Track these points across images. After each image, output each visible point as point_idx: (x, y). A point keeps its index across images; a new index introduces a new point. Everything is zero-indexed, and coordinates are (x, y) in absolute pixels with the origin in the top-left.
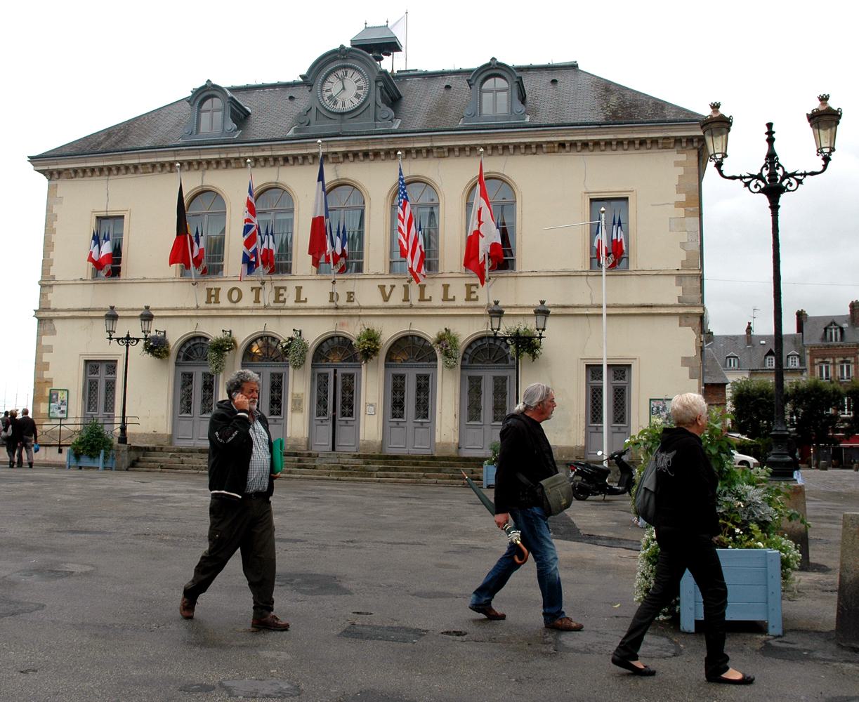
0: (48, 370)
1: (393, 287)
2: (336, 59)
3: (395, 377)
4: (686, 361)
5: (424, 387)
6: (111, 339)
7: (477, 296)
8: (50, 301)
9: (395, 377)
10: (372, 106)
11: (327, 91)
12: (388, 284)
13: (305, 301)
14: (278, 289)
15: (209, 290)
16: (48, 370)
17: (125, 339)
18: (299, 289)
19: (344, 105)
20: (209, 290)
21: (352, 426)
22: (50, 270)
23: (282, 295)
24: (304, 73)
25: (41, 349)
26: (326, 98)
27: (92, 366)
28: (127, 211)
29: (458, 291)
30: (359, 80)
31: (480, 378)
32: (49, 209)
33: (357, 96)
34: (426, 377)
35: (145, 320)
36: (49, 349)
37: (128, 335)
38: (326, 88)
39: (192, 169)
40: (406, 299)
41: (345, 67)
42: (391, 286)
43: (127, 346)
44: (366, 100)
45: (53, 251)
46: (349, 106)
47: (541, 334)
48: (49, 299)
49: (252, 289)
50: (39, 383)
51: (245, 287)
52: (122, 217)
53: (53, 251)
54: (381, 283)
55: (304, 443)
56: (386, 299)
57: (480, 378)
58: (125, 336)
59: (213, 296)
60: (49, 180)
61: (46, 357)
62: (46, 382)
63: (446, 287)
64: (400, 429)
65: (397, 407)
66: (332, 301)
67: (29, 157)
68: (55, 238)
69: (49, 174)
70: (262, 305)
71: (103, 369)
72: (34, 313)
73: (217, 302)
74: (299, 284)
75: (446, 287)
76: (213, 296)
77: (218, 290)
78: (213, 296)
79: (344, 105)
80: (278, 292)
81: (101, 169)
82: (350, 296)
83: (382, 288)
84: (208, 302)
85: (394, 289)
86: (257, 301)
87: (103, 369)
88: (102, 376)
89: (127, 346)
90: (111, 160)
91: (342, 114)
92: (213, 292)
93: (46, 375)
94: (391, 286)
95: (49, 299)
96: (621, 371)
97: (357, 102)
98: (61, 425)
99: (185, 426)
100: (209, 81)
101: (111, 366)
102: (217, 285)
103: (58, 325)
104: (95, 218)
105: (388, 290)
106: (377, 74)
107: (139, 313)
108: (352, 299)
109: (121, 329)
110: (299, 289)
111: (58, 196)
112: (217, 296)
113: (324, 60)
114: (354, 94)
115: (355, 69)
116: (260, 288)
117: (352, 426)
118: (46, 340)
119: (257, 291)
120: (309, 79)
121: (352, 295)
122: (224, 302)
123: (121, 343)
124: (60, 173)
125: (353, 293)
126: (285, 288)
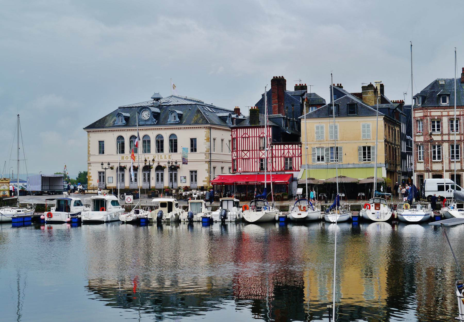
4: (206, 170)
5: (162, 175)
27: (100, 173)
29: (167, 156)
68: (90, 146)
71: (102, 173)
78: (123, 158)
87: (102, 173)
96: (196, 172)
97: (148, 118)
101: (103, 173)
103: (92, 164)
118: (90, 168)
122: (125, 159)
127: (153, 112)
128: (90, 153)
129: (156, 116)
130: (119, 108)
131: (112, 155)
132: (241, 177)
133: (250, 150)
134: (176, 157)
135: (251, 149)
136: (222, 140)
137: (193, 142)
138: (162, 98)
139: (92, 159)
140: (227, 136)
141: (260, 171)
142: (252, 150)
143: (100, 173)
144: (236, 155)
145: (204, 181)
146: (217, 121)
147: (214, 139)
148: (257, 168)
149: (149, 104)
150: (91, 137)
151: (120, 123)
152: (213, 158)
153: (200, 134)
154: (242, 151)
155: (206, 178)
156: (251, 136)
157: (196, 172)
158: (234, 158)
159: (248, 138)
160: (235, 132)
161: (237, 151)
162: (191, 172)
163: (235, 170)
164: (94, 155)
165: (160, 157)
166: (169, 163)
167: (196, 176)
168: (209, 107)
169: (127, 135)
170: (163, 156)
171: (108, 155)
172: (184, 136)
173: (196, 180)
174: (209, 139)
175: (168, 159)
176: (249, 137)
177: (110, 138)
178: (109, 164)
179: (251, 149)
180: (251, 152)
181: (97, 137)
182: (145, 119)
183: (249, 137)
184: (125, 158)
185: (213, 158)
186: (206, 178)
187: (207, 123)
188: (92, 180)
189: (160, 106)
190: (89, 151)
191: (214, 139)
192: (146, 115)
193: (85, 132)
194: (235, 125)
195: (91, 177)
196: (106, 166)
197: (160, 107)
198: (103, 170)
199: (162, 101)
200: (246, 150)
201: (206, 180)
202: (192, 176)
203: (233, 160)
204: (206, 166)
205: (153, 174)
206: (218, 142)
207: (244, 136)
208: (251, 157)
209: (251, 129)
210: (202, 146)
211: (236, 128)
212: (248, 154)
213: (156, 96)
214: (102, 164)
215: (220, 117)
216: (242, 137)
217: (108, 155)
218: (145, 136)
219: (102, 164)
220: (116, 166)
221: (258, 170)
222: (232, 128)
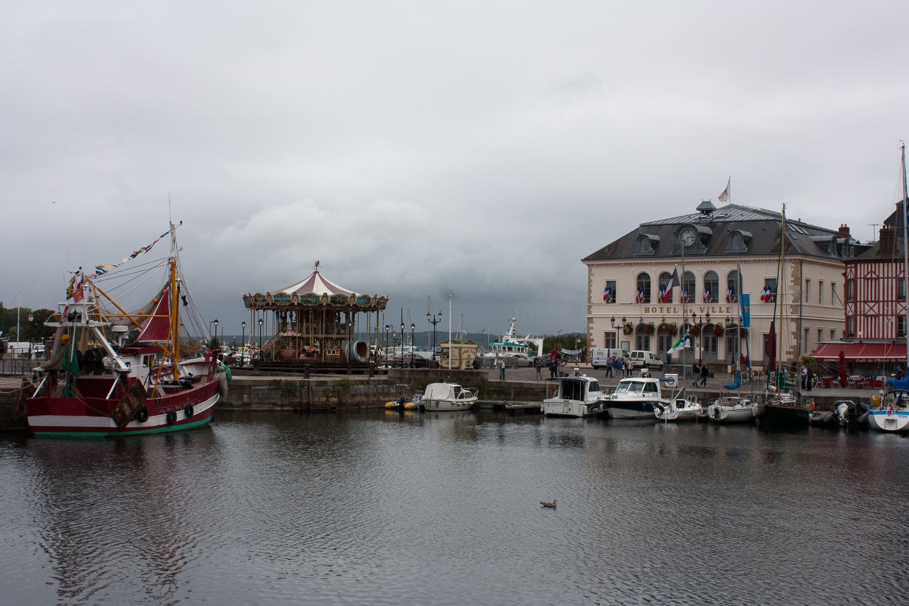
27: (607, 334)
29: (724, 309)
36: (592, 328)
88: (611, 338)
101: (614, 334)
118: (591, 325)
119: (661, 309)
122: (651, 313)
127: (703, 234)
128: (592, 300)
129: (705, 239)
130: (642, 226)
132: (860, 346)
133: (879, 302)
135: (881, 299)
136: (821, 283)
137: (771, 285)
138: (716, 209)
139: (595, 312)
140: (835, 276)
141: (897, 338)
142: (883, 301)
143: (607, 334)
144: (853, 309)
145: (788, 353)
146: (812, 249)
147: (807, 281)
148: (891, 333)
149: (692, 220)
151: (643, 252)
152: (806, 313)
153: (785, 273)
154: (864, 302)
156: (881, 276)
158: (850, 314)
159: (875, 279)
160: (853, 269)
161: (855, 303)
163: (852, 335)
166: (727, 320)
168: (797, 225)
169: (654, 273)
170: (717, 309)
172: (754, 276)
174: (798, 280)
175: (725, 314)
176: (878, 278)
177: (626, 278)
178: (624, 320)
179: (881, 299)
180: (881, 304)
181: (604, 274)
183: (878, 278)
185: (806, 313)
186: (792, 347)
187: (795, 253)
189: (711, 222)
190: (590, 298)
191: (807, 281)
192: (688, 238)
193: (585, 267)
194: (852, 257)
195: (593, 340)
196: (619, 323)
197: (711, 225)
198: (614, 330)
199: (715, 214)
200: (871, 301)
201: (791, 350)
203: (848, 318)
204: (793, 327)
206: (814, 286)
207: (869, 276)
208: (881, 313)
209: (881, 265)
210: (787, 292)
211: (855, 262)
212: (876, 308)
213: (705, 207)
214: (613, 320)
215: (816, 243)
216: (865, 278)
218: (709, 273)
219: (613, 320)
221: (894, 337)
222: (846, 262)
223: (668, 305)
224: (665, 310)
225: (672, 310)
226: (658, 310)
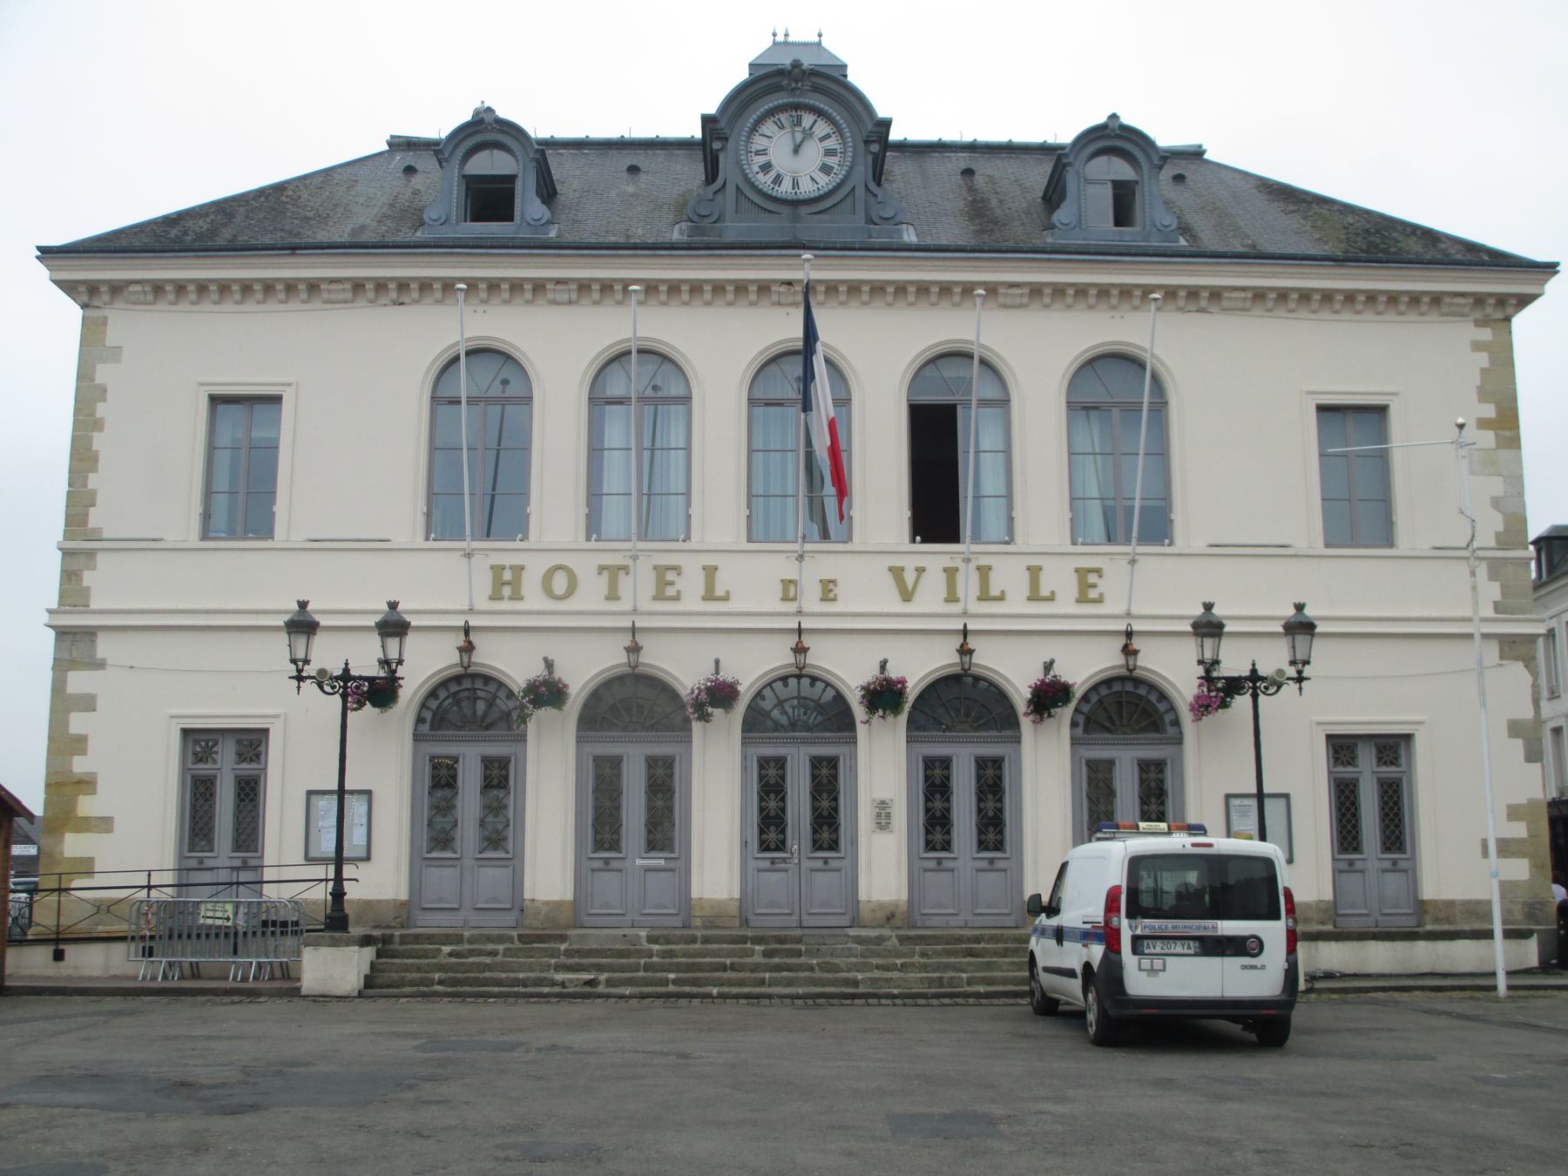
0: (83, 752)
1: (920, 571)
2: (778, 88)
3: (929, 763)
6: (300, 678)
7: (1101, 595)
8: (88, 589)
9: (929, 763)
10: (860, 192)
11: (757, 153)
12: (909, 564)
13: (726, 598)
14: (660, 571)
15: (497, 570)
16: (83, 752)
17: (337, 678)
18: (710, 571)
19: (795, 184)
20: (497, 570)
21: (839, 870)
22: (87, 515)
23: (672, 583)
24: (712, 109)
25: (63, 703)
26: (756, 168)
28: (289, 385)
29: (1060, 578)
30: (828, 136)
31: (1110, 763)
32: (85, 374)
33: (825, 169)
34: (997, 762)
35: (1204, 635)
36: (88, 703)
37: (1254, 671)
38: (754, 148)
39: (383, 301)
40: (952, 598)
41: (797, 107)
42: (917, 569)
43: (1255, 697)
44: (846, 177)
45: (96, 471)
46: (807, 189)
47: (1300, 672)
48: (85, 584)
49: (602, 569)
50: (60, 784)
51: (585, 567)
52: (276, 400)
53: (96, 471)
54: (897, 562)
55: (735, 912)
56: (907, 596)
57: (1110, 763)
58: (338, 672)
59: (508, 583)
60: (84, 306)
61: (78, 723)
62: (79, 782)
63: (1034, 572)
64: (995, 875)
65: (935, 827)
66: (785, 598)
67: (39, 248)
68: (99, 441)
69: (84, 293)
70: (625, 605)
71: (226, 756)
72: (46, 618)
73: (517, 596)
74: (710, 560)
75: (1034, 572)
76: (508, 583)
77: (518, 570)
78: (506, 583)
79: (795, 184)
80: (664, 579)
81: (381, 286)
82: (828, 589)
83: (897, 572)
84: (496, 596)
85: (924, 576)
86: (613, 596)
87: (226, 756)
89: (1255, 697)
90: (1274, 275)
91: (795, 203)
92: (507, 576)
93: (80, 765)
94: (917, 569)
95: (85, 584)
97: (825, 182)
98: (150, 887)
99: (441, 880)
100: (1114, 117)
101: (252, 743)
102: (516, 559)
104: (206, 398)
105: (909, 578)
106: (870, 126)
107: (371, 621)
108: (831, 595)
109: (327, 654)
110: (710, 571)
111: (109, 343)
112: (516, 584)
113: (745, 94)
114: (818, 163)
115: (820, 113)
116: (625, 568)
117: (839, 870)
118: (78, 682)
119: (613, 573)
120: (722, 124)
121: (831, 586)
122: (534, 598)
123: (328, 689)
124: (117, 289)
125: (833, 581)
126: (676, 569)
128: (95, 519)
130: (400, 145)
131: (379, 546)
134: (1150, 602)
139: (113, 588)
150: (116, 353)
155: (1514, 813)
157: (1392, 747)
162: (1342, 747)
164: (151, 545)
165: (968, 585)
167: (1394, 801)
171: (317, 545)
173: (1396, 834)
182: (785, 189)
184: (531, 583)
186: (1514, 813)
188: (104, 824)
201: (1519, 830)
202: (1345, 799)
205: (882, 766)
217: (317, 545)
220: (424, 663)
223: (659, 553)
224: (638, 590)
225: (690, 584)
226: (591, 595)
